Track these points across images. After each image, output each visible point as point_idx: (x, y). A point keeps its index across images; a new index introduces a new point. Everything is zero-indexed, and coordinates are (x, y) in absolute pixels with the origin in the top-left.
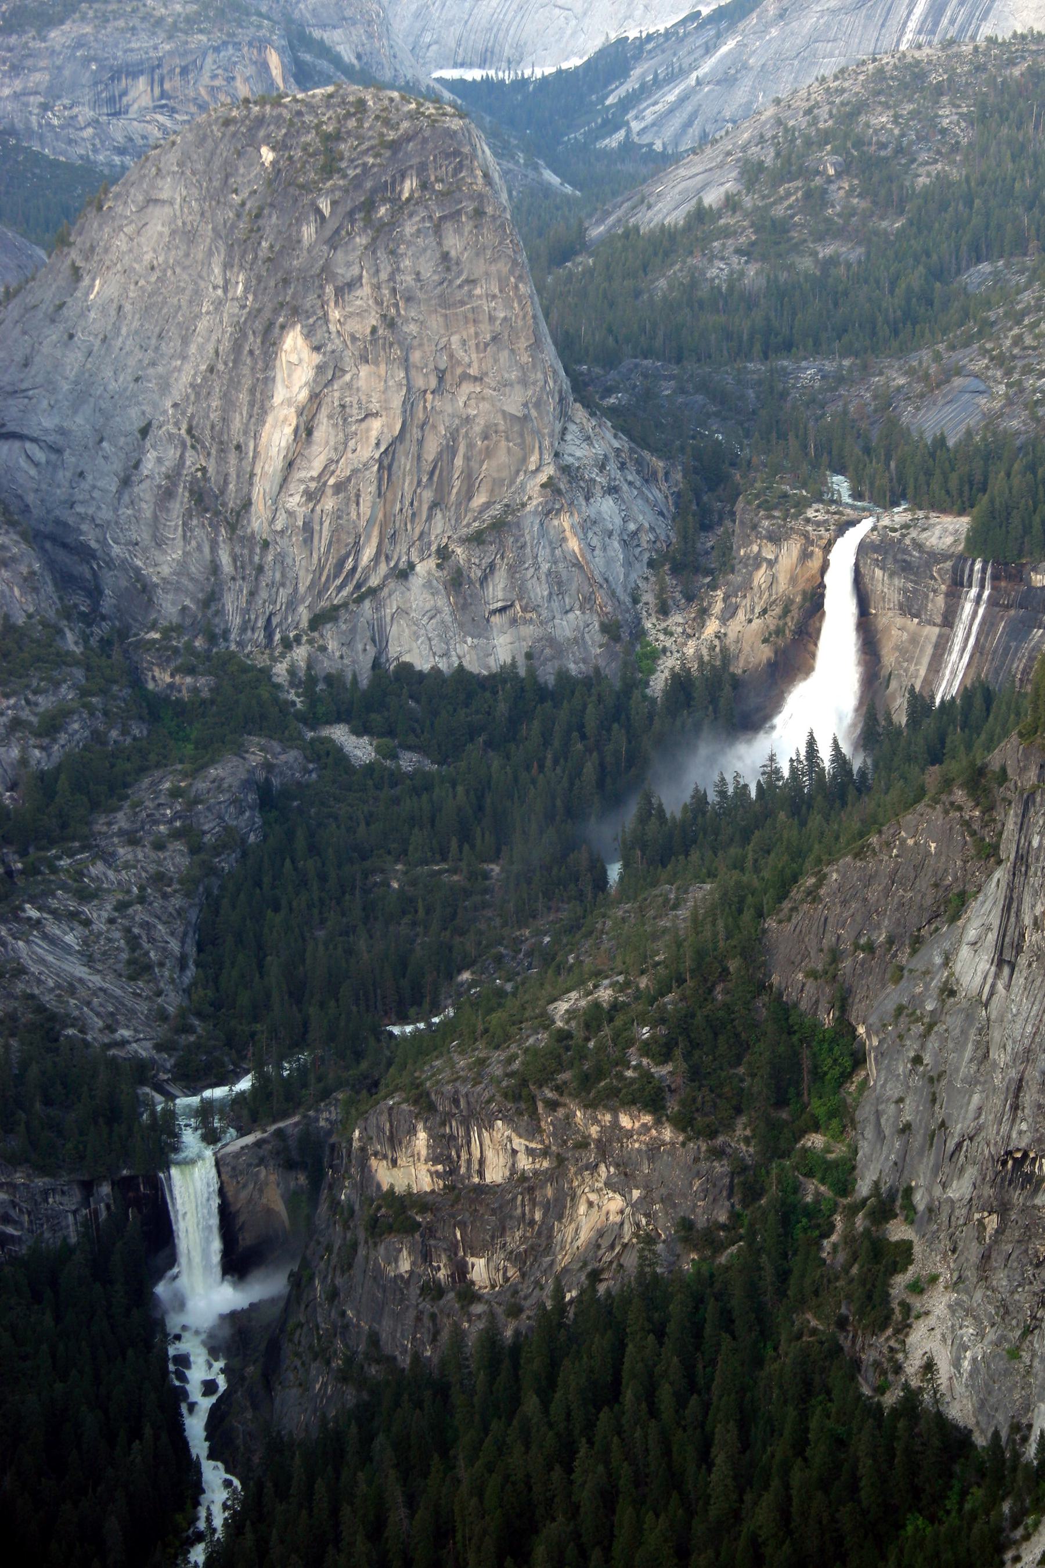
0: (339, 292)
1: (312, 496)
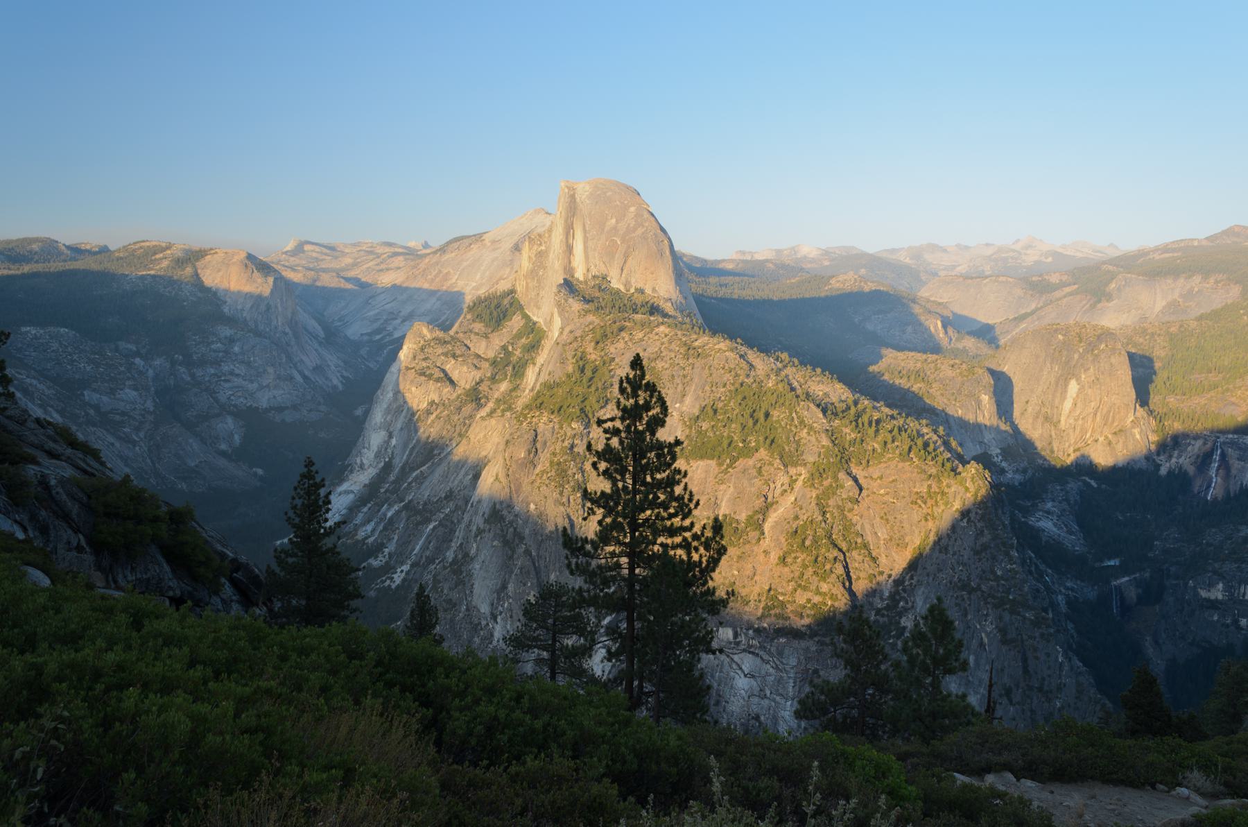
0: (1085, 371)
1: (1075, 420)
